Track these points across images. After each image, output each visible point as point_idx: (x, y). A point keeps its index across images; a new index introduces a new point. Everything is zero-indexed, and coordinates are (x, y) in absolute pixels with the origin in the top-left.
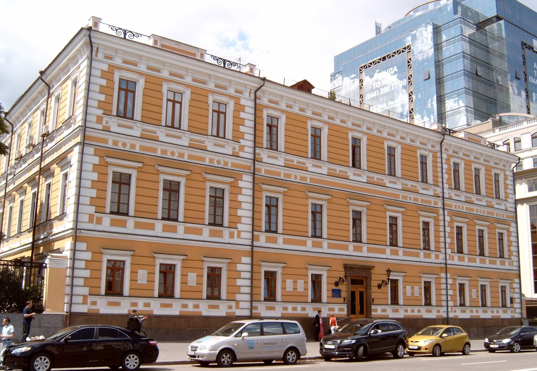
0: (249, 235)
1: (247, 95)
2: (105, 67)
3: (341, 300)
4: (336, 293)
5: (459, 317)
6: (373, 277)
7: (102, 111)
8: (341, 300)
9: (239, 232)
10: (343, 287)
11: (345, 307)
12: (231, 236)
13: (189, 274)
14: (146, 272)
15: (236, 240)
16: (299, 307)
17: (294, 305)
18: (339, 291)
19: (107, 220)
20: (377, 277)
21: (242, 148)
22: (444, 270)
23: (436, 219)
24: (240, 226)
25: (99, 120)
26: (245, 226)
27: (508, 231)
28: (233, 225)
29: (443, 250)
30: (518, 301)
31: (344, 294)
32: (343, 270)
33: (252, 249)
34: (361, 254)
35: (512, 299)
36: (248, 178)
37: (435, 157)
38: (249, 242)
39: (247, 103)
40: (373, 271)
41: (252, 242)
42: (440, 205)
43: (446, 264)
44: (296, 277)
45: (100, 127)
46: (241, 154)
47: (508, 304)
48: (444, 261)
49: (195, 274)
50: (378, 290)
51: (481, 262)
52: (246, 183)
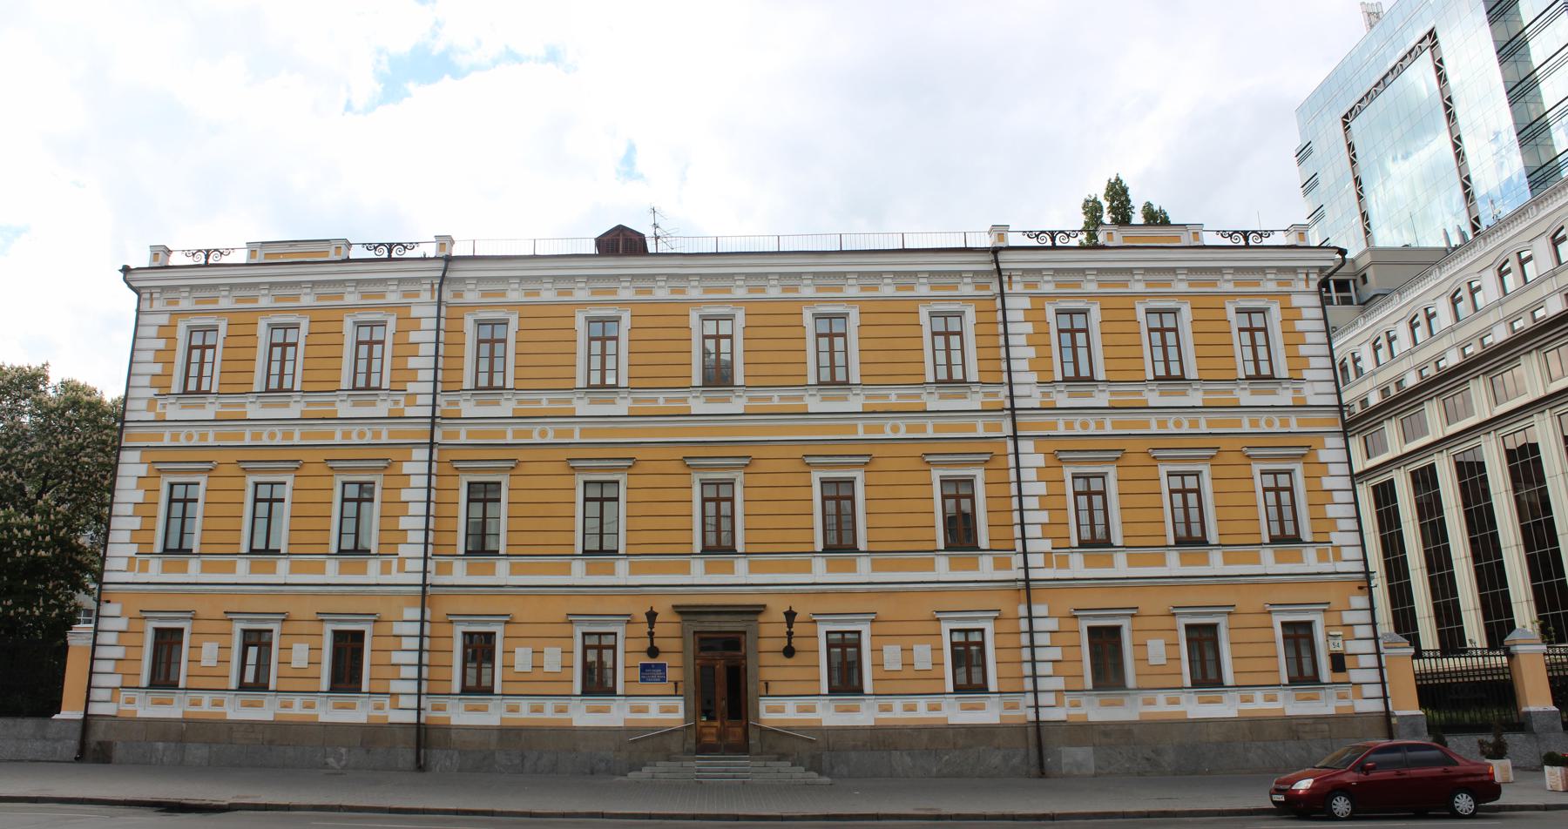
0: (419, 565)
1: (426, 296)
2: (164, 319)
3: (668, 688)
5: (1190, 716)
7: (156, 391)
8: (668, 688)
9: (402, 561)
11: (679, 703)
12: (386, 569)
13: (296, 646)
14: (216, 645)
15: (395, 577)
16: (549, 706)
17: (537, 701)
18: (662, 667)
19: (155, 564)
20: (771, 630)
21: (411, 398)
22: (1023, 594)
24: (403, 550)
25: (151, 404)
26: (411, 550)
28: (388, 551)
31: (672, 674)
32: (678, 618)
33: (424, 592)
36: (423, 454)
38: (418, 579)
39: (424, 310)
40: (761, 618)
41: (425, 578)
44: (906, 639)
45: (151, 416)
46: (409, 412)
48: (1021, 575)
49: (306, 646)
50: (789, 661)
51: (997, 567)
52: (416, 465)
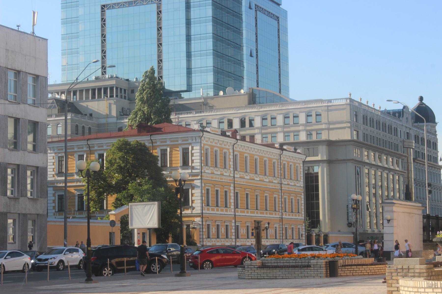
4: (252, 235)
6: (262, 226)
8: (253, 237)
10: (254, 231)
23: (279, 195)
27: (301, 198)
29: (281, 211)
30: (304, 235)
34: (258, 215)
35: (302, 234)
36: (232, 185)
37: (278, 162)
42: (279, 188)
43: (282, 218)
47: (301, 238)
52: (232, 188)
